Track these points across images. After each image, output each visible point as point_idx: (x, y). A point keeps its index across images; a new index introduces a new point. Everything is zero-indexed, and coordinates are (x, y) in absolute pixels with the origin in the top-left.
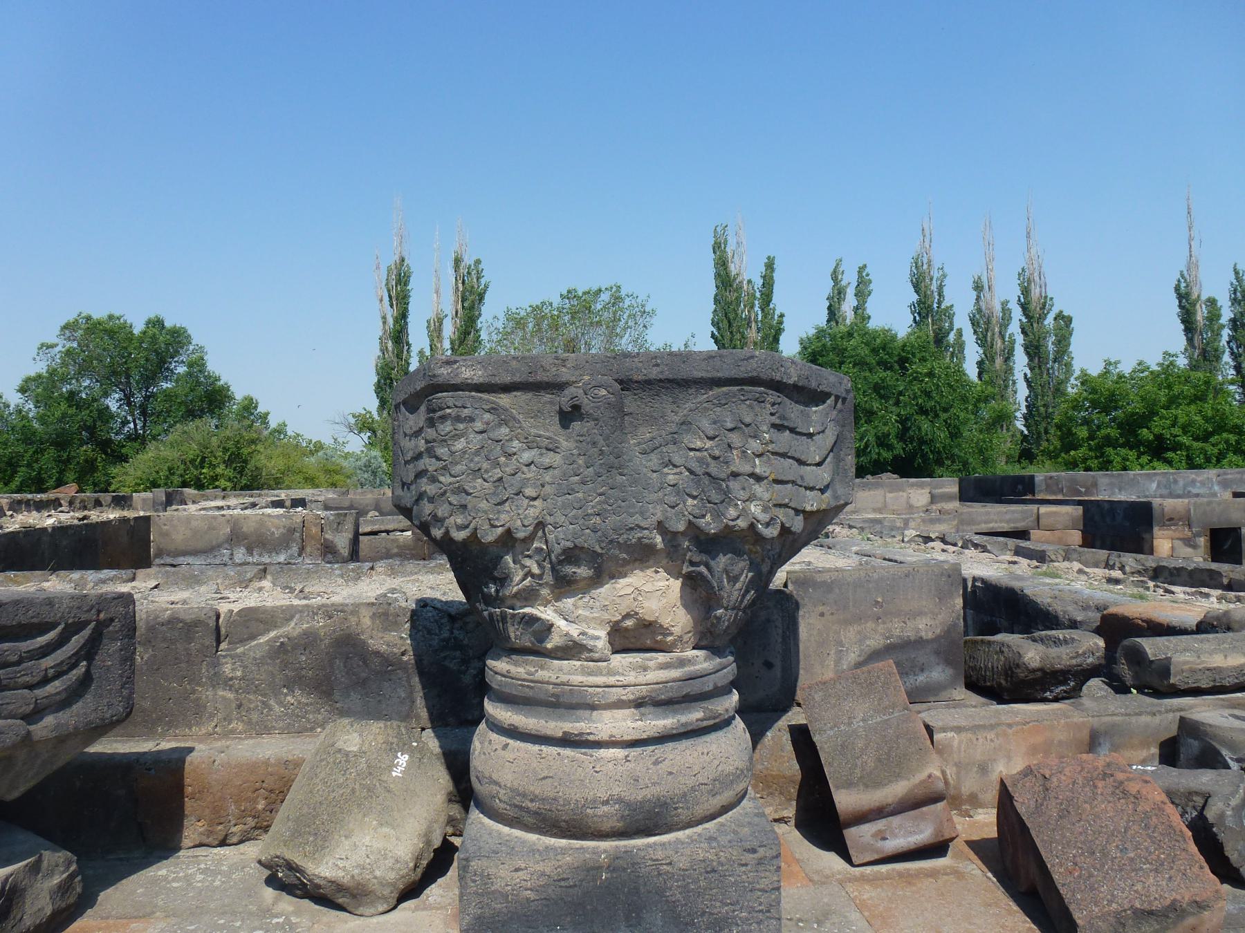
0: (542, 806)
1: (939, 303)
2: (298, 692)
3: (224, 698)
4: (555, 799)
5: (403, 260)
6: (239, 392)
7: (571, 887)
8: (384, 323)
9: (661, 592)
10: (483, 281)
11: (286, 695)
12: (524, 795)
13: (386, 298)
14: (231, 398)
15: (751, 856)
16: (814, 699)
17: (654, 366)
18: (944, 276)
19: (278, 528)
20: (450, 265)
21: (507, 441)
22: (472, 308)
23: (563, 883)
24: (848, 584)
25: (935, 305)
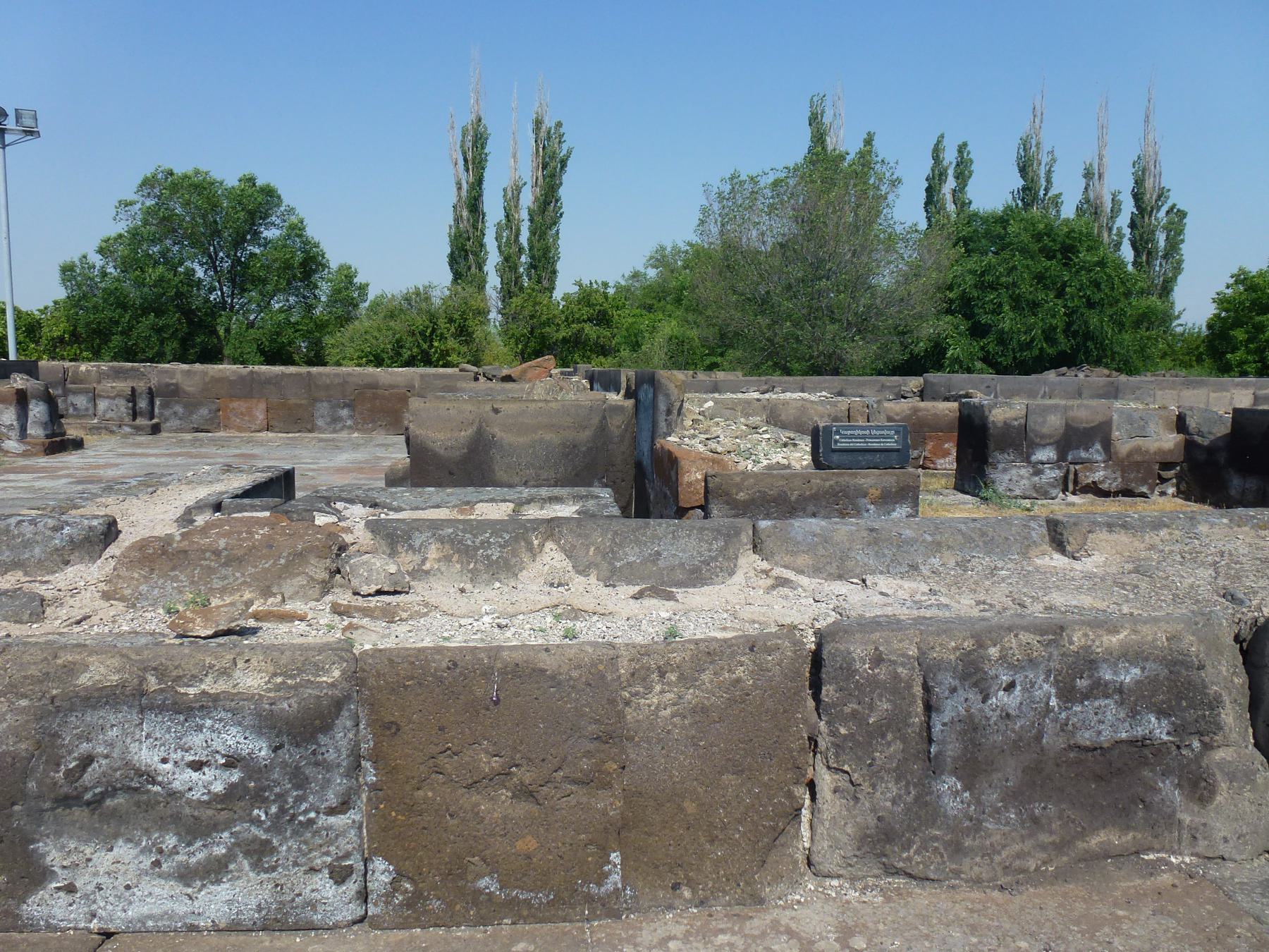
1: (1047, 190)
5: (480, 120)
6: (335, 257)
8: (459, 189)
10: (565, 147)
13: (461, 162)
14: (324, 266)
18: (1054, 160)
19: (822, 417)
20: (530, 126)
22: (553, 176)
25: (1042, 192)
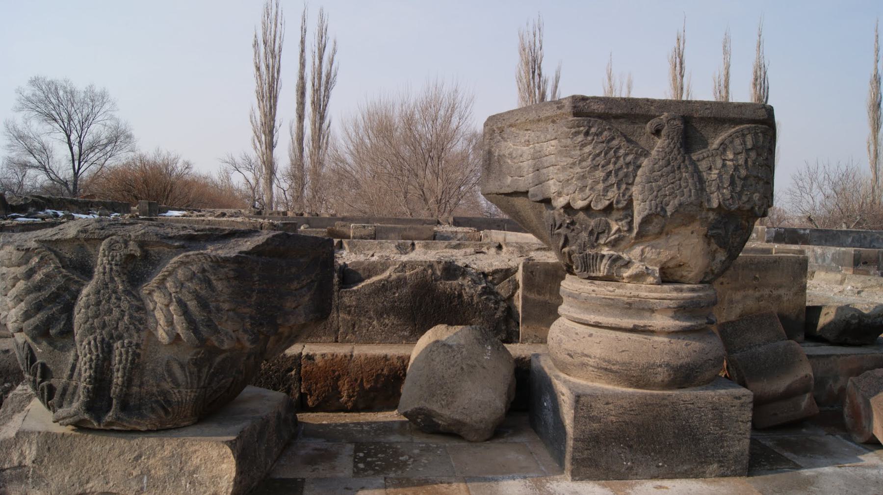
0: (620, 368)
2: (392, 317)
3: (344, 319)
4: (630, 363)
7: (637, 415)
9: (693, 245)
11: (384, 319)
12: (609, 362)
15: (739, 401)
16: (727, 332)
17: (706, 109)
21: (617, 148)
23: (632, 413)
24: (739, 264)
